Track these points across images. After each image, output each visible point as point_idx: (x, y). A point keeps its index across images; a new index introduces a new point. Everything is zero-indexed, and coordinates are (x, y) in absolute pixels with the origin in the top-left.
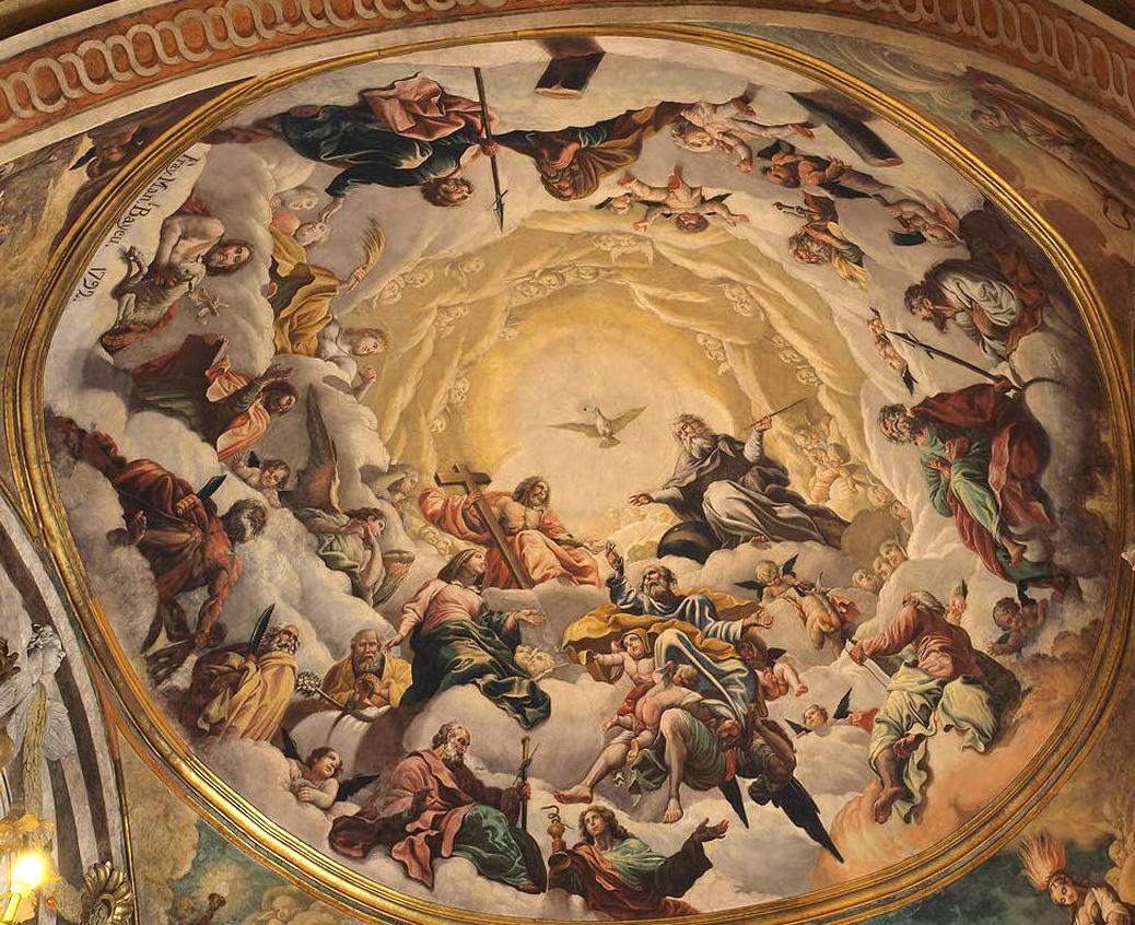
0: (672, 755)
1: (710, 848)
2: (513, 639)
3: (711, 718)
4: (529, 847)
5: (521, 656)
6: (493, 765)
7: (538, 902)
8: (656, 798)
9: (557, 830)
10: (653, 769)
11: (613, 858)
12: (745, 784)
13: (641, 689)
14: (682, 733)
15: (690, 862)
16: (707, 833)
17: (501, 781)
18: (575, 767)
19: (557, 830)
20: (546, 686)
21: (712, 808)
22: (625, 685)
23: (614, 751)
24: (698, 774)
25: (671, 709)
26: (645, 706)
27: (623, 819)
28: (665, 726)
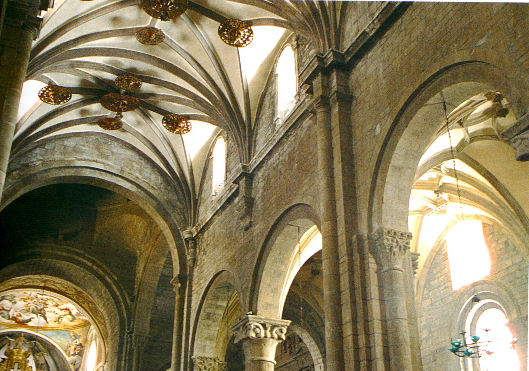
0: (31, 310)
1: (32, 319)
2: (15, 297)
3: (37, 308)
4: (9, 316)
5: (15, 298)
6: (7, 307)
7: (9, 321)
8: (27, 313)
9: (13, 314)
10: (28, 311)
11: (20, 318)
12: (39, 314)
13: (29, 303)
14: (33, 308)
15: (30, 320)
16: (33, 318)
17: (8, 309)
18: (18, 309)
19: (13, 314)
20: (17, 302)
21: (34, 315)
22: (27, 303)
23: (23, 308)
24: (33, 312)
25: (32, 306)
26: (29, 305)
27: (22, 315)
28: (31, 307)
